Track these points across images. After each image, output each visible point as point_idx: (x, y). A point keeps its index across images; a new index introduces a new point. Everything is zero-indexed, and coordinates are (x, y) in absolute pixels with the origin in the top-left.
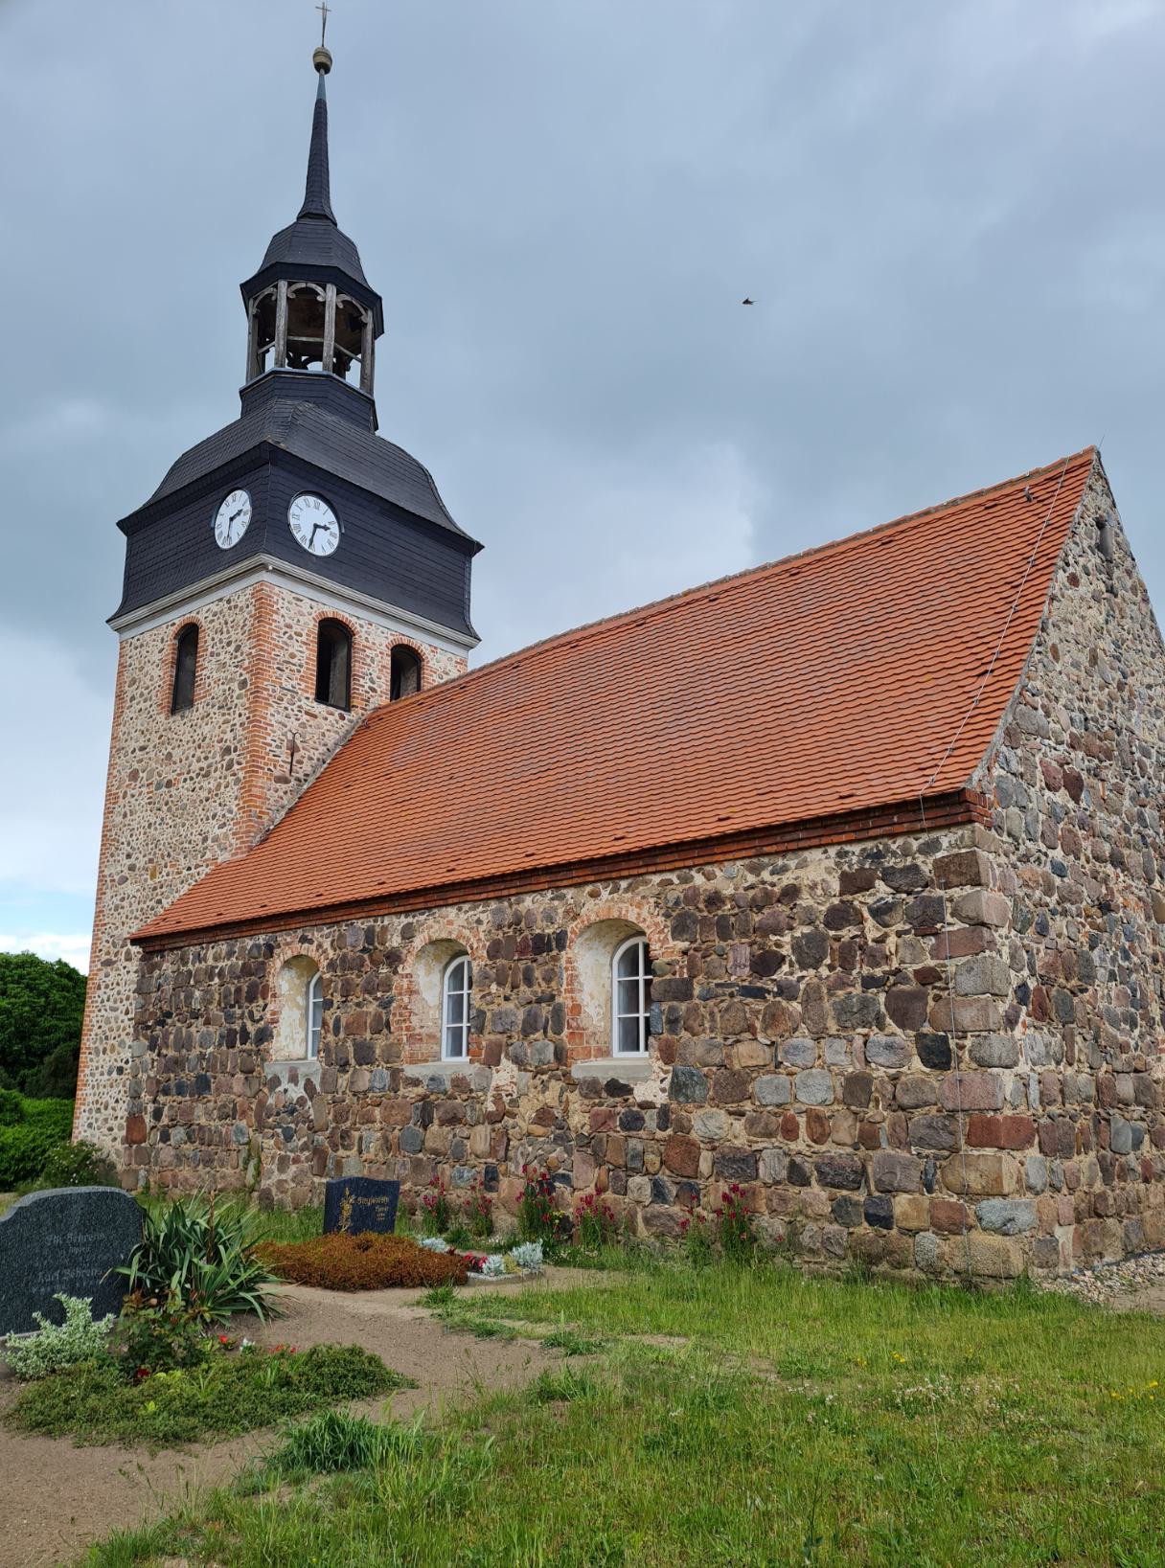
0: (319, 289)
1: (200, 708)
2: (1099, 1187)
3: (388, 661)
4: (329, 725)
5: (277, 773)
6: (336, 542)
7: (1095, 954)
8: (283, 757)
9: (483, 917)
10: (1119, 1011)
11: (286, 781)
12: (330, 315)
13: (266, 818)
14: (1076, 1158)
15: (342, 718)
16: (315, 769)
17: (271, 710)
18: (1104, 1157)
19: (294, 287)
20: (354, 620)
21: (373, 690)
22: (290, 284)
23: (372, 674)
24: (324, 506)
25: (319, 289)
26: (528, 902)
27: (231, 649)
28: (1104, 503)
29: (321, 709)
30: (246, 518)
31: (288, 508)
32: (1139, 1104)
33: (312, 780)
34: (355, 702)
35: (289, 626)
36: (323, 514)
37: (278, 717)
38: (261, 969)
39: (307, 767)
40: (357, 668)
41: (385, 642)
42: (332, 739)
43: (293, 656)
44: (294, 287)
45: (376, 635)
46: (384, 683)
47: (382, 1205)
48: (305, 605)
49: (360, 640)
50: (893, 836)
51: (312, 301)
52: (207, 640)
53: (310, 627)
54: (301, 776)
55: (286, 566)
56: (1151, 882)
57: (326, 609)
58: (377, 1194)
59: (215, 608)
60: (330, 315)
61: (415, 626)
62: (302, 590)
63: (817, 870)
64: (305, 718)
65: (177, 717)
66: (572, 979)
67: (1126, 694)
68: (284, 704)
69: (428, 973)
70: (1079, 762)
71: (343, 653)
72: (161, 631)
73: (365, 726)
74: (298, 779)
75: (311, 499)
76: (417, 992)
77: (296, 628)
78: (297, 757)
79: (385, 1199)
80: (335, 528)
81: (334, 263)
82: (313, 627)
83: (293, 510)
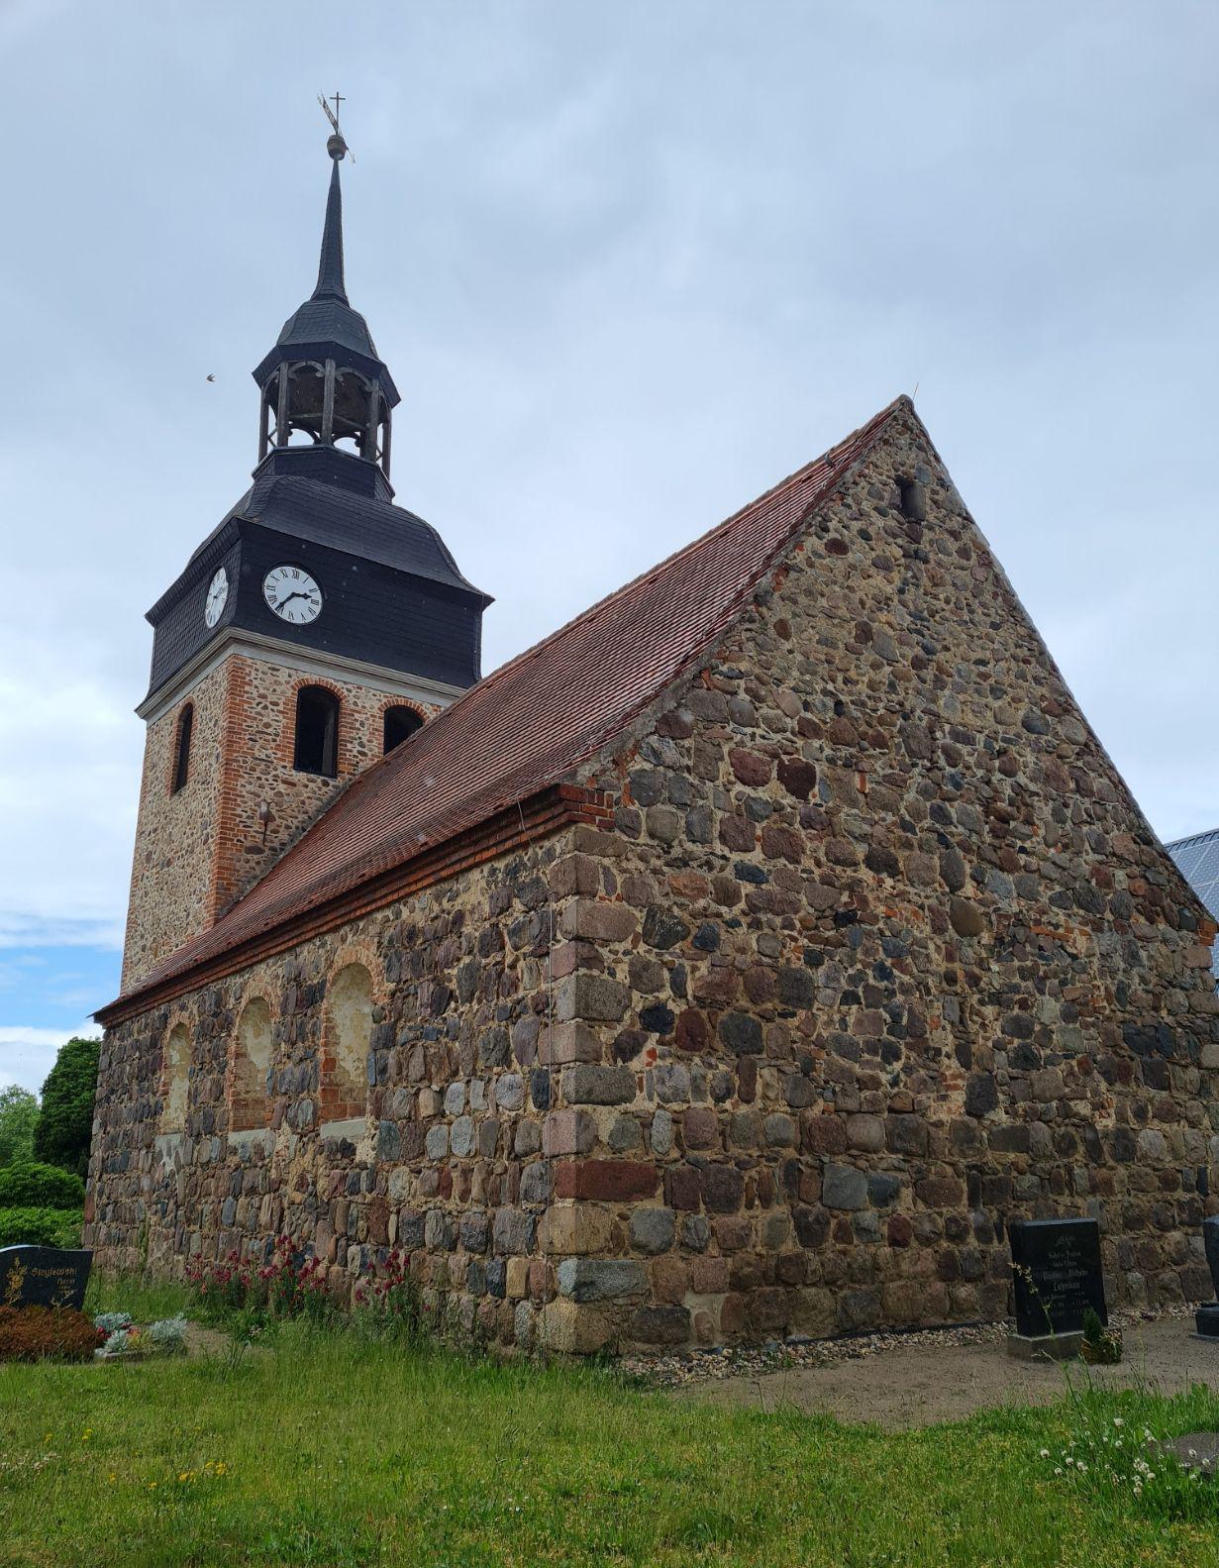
0: (318, 366)
1: (191, 785)
2: (790, 1246)
3: (380, 724)
4: (312, 789)
5: (248, 843)
6: (318, 609)
7: (819, 975)
8: (256, 828)
9: (280, 971)
10: (860, 1040)
11: (259, 851)
12: (329, 388)
13: (234, 890)
14: (743, 1212)
15: (326, 784)
16: (292, 838)
17: (242, 781)
18: (805, 1214)
19: (294, 368)
20: (339, 685)
21: (364, 754)
22: (291, 365)
23: (362, 737)
24: (303, 575)
25: (318, 366)
26: (306, 953)
27: (211, 725)
28: (912, 458)
29: (301, 777)
30: (224, 595)
31: (262, 580)
32: (893, 1150)
33: (289, 848)
34: (341, 767)
35: (264, 697)
36: (305, 583)
37: (249, 787)
38: (155, 1043)
39: (284, 836)
40: (344, 733)
41: (377, 705)
42: (312, 806)
43: (267, 725)
44: (294, 368)
45: (366, 696)
46: (376, 746)
47: (69, 1277)
48: (283, 675)
49: (348, 704)
50: (525, 846)
51: (325, 377)
52: (199, 715)
53: (287, 694)
54: (276, 844)
55: (257, 637)
56: (955, 887)
57: (307, 676)
58: (58, 1265)
59: (203, 686)
60: (329, 388)
61: (406, 684)
62: (276, 660)
63: (475, 891)
64: (282, 788)
65: (176, 797)
66: (330, 1030)
67: (929, 673)
68: (257, 774)
69: (257, 1035)
70: (816, 752)
71: (332, 714)
72: (170, 715)
73: (349, 793)
74: (273, 849)
75: (289, 570)
76: (244, 1055)
77: (272, 698)
78: (271, 826)
79: (70, 1271)
80: (317, 596)
81: (331, 338)
82: (291, 694)
83: (269, 581)
